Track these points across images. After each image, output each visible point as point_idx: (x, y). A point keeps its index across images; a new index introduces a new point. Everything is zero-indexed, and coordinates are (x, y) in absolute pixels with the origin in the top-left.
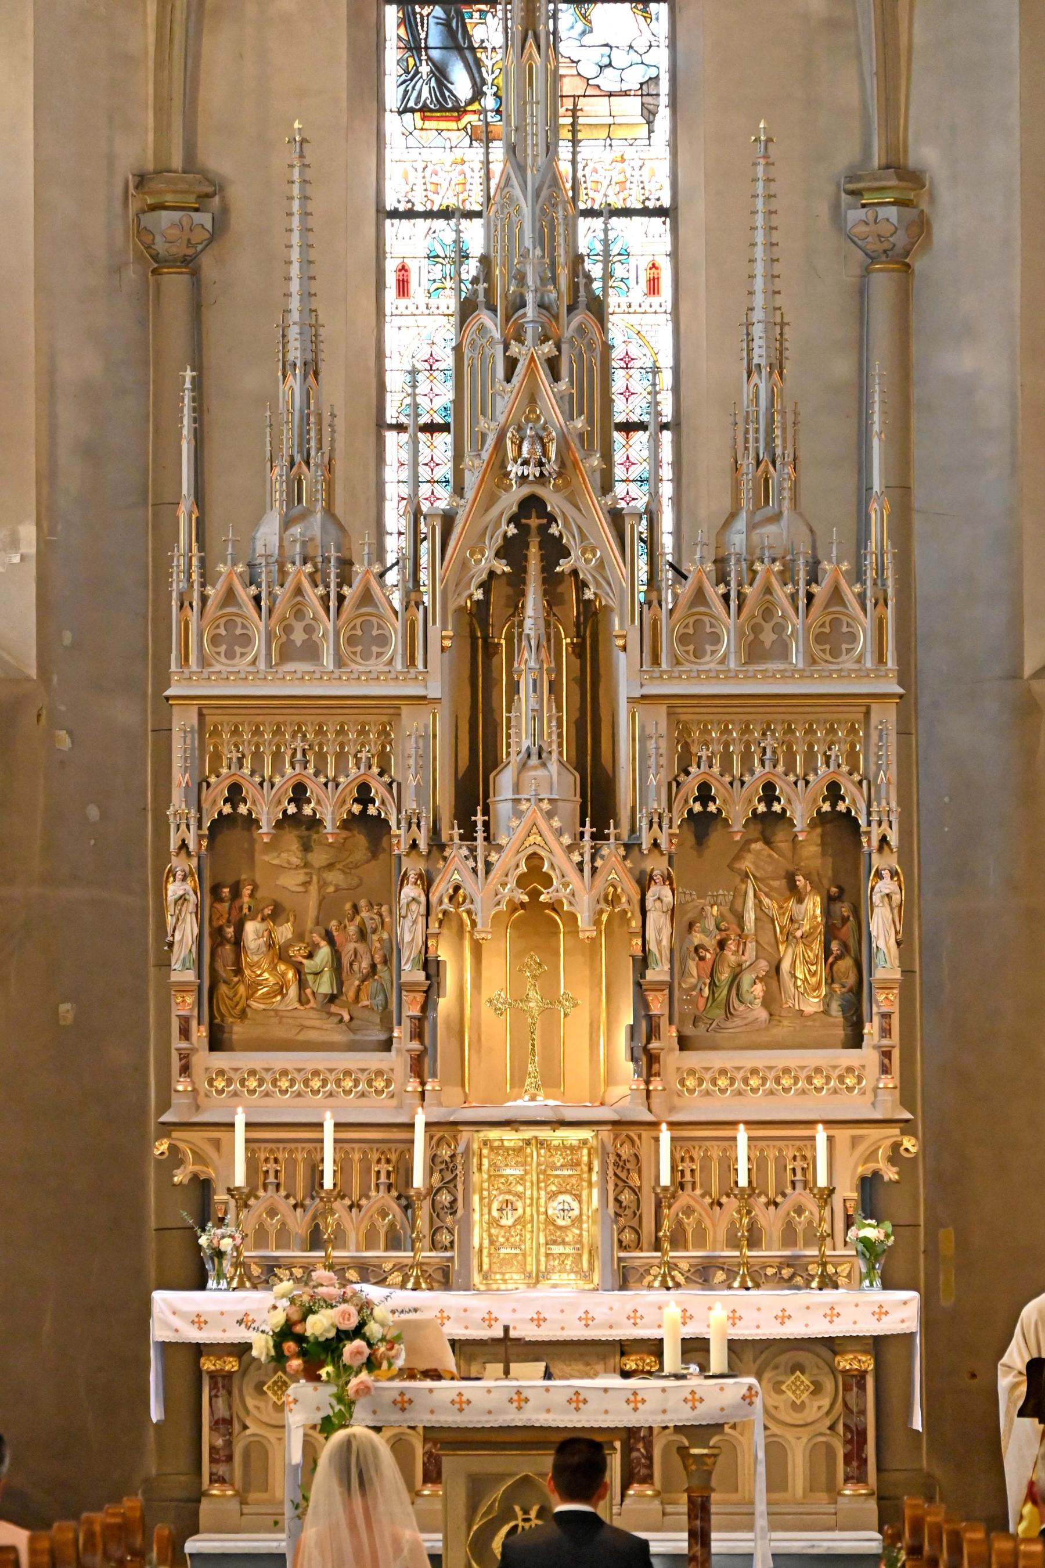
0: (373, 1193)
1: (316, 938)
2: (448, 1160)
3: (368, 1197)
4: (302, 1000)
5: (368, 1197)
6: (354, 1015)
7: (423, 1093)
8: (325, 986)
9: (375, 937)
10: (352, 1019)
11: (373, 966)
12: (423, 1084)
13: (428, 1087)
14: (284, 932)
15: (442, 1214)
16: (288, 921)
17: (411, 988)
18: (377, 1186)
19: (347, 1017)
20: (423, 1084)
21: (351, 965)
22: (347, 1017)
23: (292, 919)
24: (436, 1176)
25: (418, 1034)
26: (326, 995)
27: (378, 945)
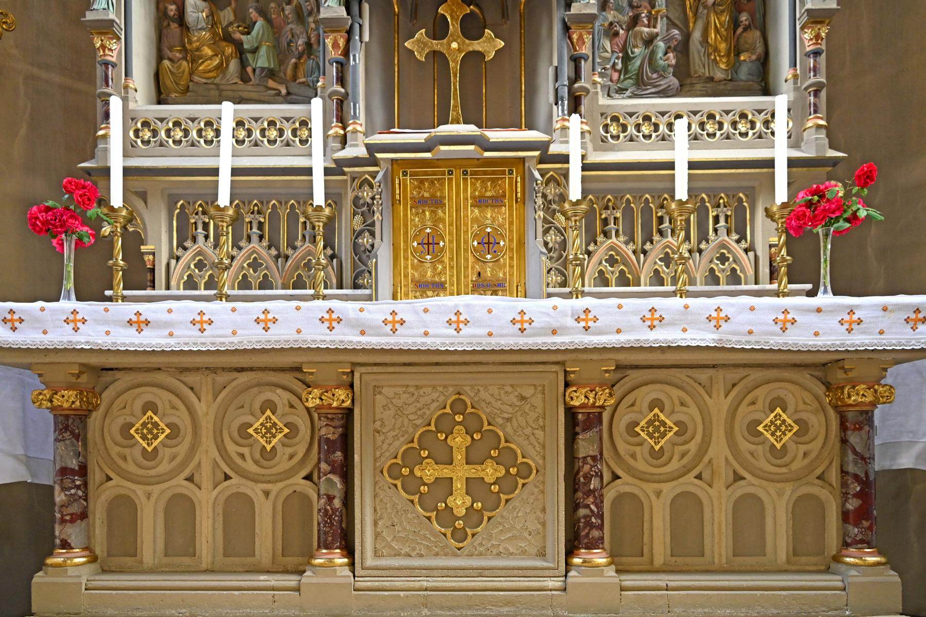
0: (298, 243)
1: (253, 13)
2: (369, 200)
3: (295, 248)
4: (245, 79)
5: (295, 248)
6: (292, 91)
7: (345, 136)
8: (263, 60)
9: (311, 19)
10: (288, 93)
11: (309, 45)
12: (344, 128)
13: (349, 128)
14: (227, 15)
15: (364, 257)
16: (230, 4)
17: (332, 25)
18: (304, 236)
19: (284, 91)
20: (344, 128)
21: (289, 44)
22: (284, 91)
23: (233, 5)
24: (358, 218)
25: (341, 80)
26: (263, 69)
27: (313, 26)
